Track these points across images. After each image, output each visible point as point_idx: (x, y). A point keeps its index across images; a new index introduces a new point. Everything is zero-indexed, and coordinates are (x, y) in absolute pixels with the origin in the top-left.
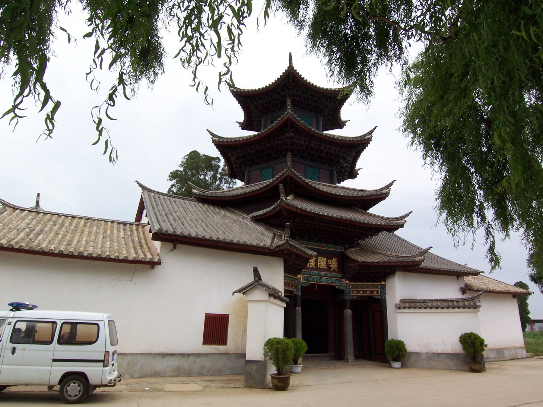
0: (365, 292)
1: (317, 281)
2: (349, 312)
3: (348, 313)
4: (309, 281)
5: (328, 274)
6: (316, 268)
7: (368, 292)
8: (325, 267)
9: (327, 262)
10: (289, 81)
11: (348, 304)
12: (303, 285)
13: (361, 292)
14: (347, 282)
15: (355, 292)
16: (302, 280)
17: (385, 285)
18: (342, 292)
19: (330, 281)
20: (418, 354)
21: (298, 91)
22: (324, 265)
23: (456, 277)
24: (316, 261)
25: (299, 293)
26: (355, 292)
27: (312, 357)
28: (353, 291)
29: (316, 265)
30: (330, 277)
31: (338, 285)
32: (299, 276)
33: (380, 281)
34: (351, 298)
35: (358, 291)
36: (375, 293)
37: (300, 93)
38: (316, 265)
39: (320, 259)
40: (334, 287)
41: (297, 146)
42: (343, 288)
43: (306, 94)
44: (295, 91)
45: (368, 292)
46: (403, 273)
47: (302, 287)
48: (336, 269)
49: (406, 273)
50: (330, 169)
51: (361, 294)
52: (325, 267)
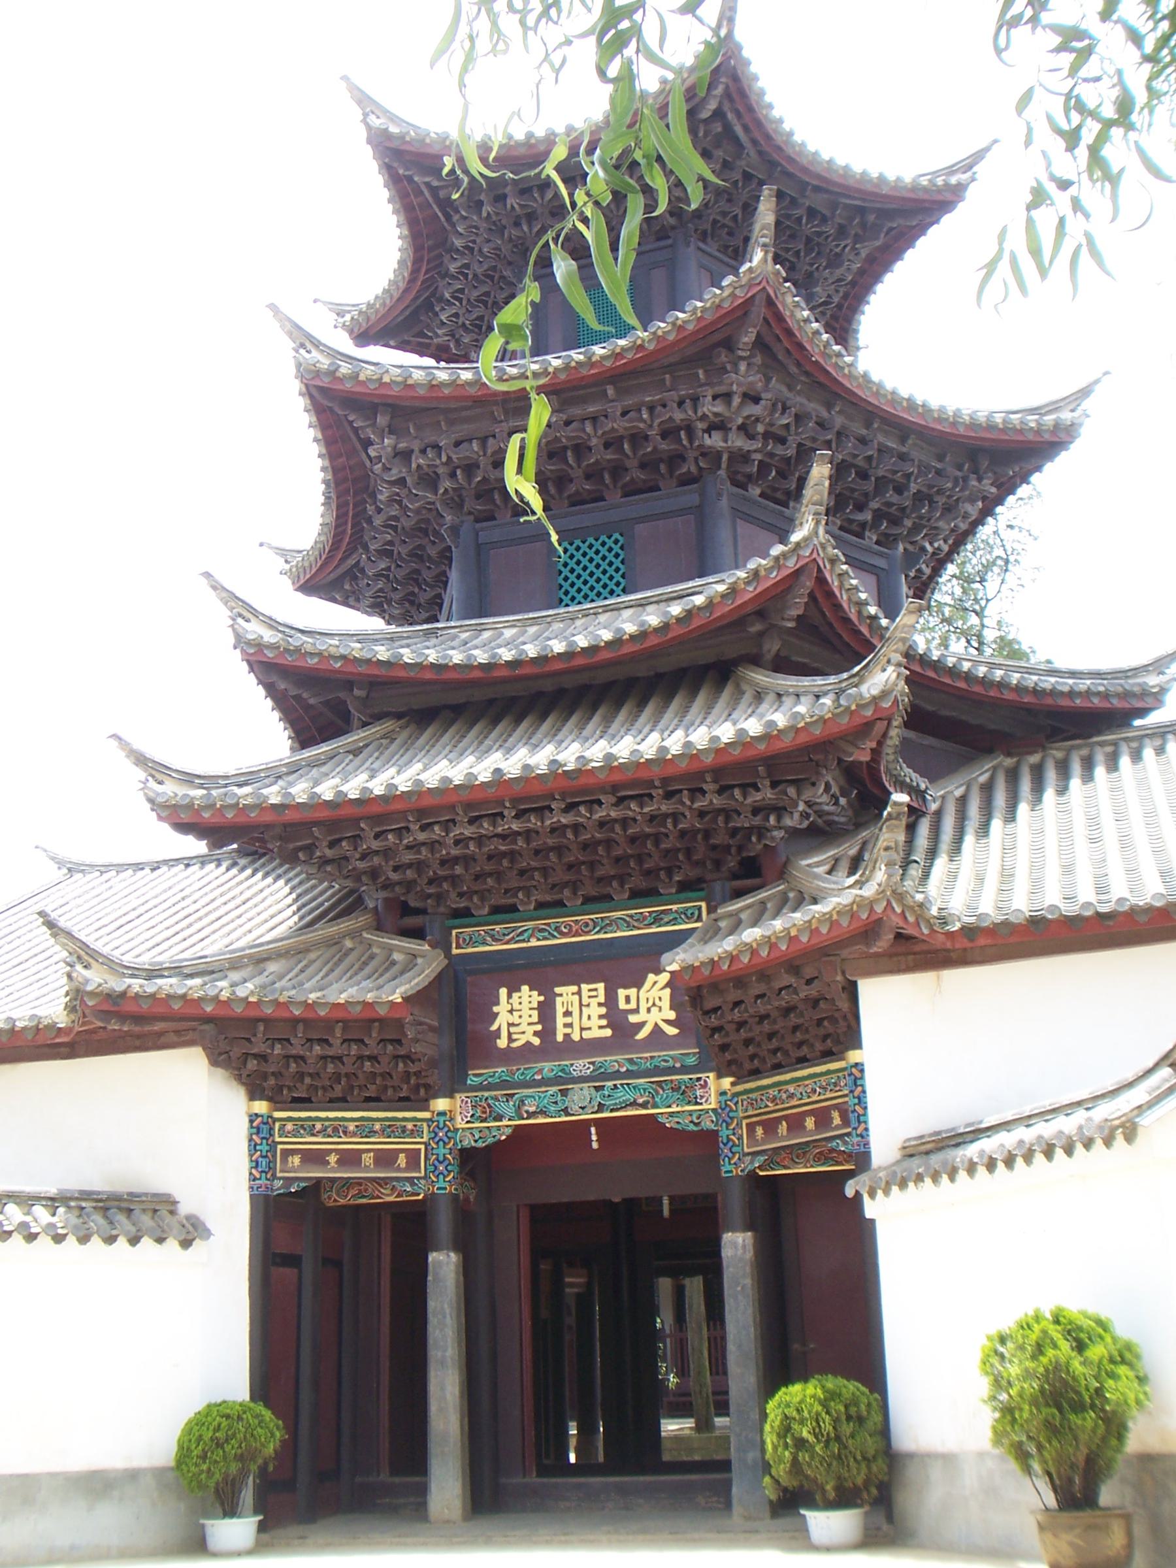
0: (796, 1123)
1: (543, 1112)
3: (727, 1253)
4: (499, 1118)
5: (614, 1061)
6: (549, 1044)
7: (810, 1123)
8: (598, 1030)
9: (610, 1001)
11: (734, 1203)
12: (468, 1142)
13: (783, 1128)
14: (727, 1082)
15: (759, 1131)
16: (460, 1123)
19: (622, 1096)
22: (596, 1022)
24: (546, 1012)
25: (445, 1184)
26: (759, 1131)
27: (622, 1491)
28: (751, 1128)
30: (630, 1074)
31: (671, 1112)
32: (441, 1104)
34: (749, 1165)
35: (770, 1127)
36: (837, 1121)
37: (511, 201)
39: (566, 995)
40: (647, 1129)
41: (453, 475)
42: (707, 1124)
44: (487, 209)
45: (810, 1123)
47: (467, 1156)
48: (672, 1031)
50: (695, 499)
51: (784, 1137)
52: (598, 1030)
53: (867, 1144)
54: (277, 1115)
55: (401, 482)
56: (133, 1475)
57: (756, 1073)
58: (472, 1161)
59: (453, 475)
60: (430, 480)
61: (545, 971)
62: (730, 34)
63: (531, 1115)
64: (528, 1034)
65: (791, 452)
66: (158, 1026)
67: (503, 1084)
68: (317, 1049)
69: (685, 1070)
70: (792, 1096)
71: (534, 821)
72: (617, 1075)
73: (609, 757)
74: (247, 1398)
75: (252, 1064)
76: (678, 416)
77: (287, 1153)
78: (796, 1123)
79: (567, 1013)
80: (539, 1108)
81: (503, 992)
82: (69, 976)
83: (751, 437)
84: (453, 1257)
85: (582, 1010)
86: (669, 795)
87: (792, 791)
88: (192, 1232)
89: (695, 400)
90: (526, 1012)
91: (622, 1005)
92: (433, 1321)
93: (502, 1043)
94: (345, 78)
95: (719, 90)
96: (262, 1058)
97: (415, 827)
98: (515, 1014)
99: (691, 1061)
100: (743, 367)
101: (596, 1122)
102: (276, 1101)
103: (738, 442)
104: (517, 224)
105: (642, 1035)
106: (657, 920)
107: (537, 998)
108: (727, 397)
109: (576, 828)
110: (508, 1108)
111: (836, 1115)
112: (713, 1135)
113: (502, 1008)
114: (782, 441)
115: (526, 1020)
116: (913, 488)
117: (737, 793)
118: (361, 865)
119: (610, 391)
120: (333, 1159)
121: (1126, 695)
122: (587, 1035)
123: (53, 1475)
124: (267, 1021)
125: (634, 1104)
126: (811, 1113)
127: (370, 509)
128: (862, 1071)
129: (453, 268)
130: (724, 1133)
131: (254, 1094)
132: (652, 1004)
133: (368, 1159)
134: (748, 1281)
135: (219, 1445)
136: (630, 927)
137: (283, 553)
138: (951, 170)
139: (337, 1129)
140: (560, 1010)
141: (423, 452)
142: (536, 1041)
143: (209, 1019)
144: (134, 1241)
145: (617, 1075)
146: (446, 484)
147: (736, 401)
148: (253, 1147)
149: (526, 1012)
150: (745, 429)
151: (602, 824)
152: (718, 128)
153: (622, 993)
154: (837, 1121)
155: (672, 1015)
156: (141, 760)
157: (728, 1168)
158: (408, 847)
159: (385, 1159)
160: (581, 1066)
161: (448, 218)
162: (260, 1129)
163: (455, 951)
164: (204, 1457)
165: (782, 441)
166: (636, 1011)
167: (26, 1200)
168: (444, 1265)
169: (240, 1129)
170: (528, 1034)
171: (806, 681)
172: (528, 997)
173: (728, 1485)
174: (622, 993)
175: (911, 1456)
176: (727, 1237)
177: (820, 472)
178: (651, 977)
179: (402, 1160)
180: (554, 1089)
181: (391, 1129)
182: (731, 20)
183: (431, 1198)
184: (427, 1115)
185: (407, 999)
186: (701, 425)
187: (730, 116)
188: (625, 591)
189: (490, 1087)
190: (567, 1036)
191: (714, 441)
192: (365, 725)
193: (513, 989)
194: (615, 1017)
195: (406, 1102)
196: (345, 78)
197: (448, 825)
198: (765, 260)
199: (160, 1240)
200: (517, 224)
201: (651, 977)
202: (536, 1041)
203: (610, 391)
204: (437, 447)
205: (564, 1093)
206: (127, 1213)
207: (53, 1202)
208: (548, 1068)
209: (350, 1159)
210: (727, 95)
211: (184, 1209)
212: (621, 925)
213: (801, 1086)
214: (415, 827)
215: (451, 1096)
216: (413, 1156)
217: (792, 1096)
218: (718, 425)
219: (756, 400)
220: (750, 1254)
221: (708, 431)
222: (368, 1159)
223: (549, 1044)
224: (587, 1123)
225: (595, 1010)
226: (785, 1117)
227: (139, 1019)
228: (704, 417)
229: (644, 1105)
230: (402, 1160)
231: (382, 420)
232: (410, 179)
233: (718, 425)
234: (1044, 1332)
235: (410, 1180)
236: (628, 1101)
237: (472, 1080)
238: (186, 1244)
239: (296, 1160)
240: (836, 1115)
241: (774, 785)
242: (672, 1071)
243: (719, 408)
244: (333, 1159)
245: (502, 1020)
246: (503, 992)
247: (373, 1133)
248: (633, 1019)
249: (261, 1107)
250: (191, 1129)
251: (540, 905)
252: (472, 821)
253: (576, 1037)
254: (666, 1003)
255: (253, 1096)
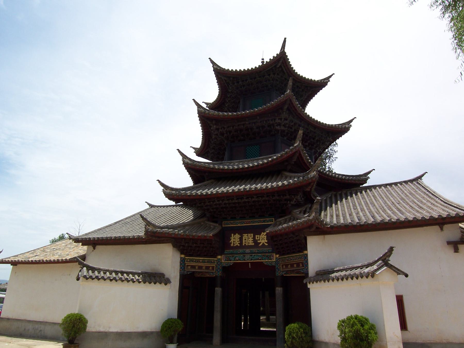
0: (292, 265)
1: (240, 260)
2: (279, 290)
3: (277, 292)
5: (255, 250)
6: (241, 246)
7: (295, 265)
8: (251, 243)
9: (254, 237)
10: (226, 80)
14: (278, 256)
15: (284, 266)
16: (223, 261)
17: (307, 255)
18: (273, 268)
20: (326, 344)
21: (238, 82)
22: (251, 242)
23: (437, 228)
24: (241, 239)
25: (219, 274)
26: (284, 266)
28: (283, 266)
29: (241, 243)
32: (219, 257)
33: (302, 252)
35: (287, 266)
36: (301, 265)
37: (240, 83)
38: (241, 243)
39: (245, 236)
41: (227, 133)
42: (273, 264)
43: (246, 80)
44: (236, 84)
45: (295, 265)
46: (322, 236)
48: (267, 244)
49: (326, 236)
51: (289, 268)
52: (251, 243)
53: (308, 271)
54: (186, 258)
55: (217, 135)
56: (152, 333)
57: (284, 254)
58: (225, 269)
59: (227, 133)
60: (222, 134)
61: (241, 231)
62: (284, 50)
63: (237, 260)
64: (237, 244)
65: (293, 130)
66: (163, 239)
67: (232, 254)
68: (195, 245)
69: (269, 253)
70: (291, 260)
71: (240, 201)
72: (255, 253)
73: (256, 188)
74: (176, 317)
75: (181, 247)
76: (271, 123)
77: (188, 266)
78: (292, 265)
79: (245, 240)
80: (239, 259)
81: (233, 235)
82: (145, 228)
83: (285, 127)
84: (220, 289)
85: (248, 239)
86: (267, 196)
87: (293, 197)
88: (167, 281)
89: (275, 120)
90: (237, 239)
91: (256, 239)
92: (216, 302)
93: (232, 245)
94: (210, 58)
95: (281, 62)
96: (184, 246)
97: (216, 201)
98: (235, 239)
99: (270, 251)
100: (284, 113)
101: (251, 262)
102: (186, 255)
103: (283, 128)
104: (241, 87)
105: (261, 245)
106: (264, 222)
107: (239, 236)
108: (281, 119)
109: (248, 202)
110: (232, 259)
111: (301, 264)
112: (274, 267)
113: (232, 238)
114: (291, 128)
115: (237, 240)
116: (316, 139)
117: (282, 197)
118: (206, 208)
119: (258, 118)
120: (197, 267)
121: (359, 180)
122: (249, 244)
123: (134, 332)
124: (185, 239)
125: (258, 259)
126: (295, 263)
127: (211, 140)
128: (307, 255)
129: (229, 96)
130: (277, 266)
131: (182, 253)
132: (263, 239)
133: (204, 268)
134: (281, 298)
135: (170, 328)
136: (258, 223)
137: (194, 148)
138: (324, 79)
139: (198, 261)
140: (244, 239)
141: (221, 129)
142: (239, 245)
143: (173, 238)
144: (155, 283)
145: (255, 253)
146: (225, 135)
147: (283, 120)
148: (181, 264)
149: (237, 239)
150: (284, 126)
151: (254, 202)
152: (280, 69)
153: (256, 236)
154: (301, 265)
155: (267, 241)
156: (162, 185)
157: (278, 274)
158: (215, 205)
159: (207, 268)
160: (248, 251)
161: (228, 86)
162: (182, 261)
163: (223, 226)
164: (166, 331)
165: (291, 128)
166: (259, 240)
167: (133, 274)
168: (218, 290)
169: (178, 260)
170: (237, 244)
171: (296, 174)
172: (237, 236)
173: (275, 341)
174: (256, 236)
175: (317, 341)
176: (277, 288)
177: (301, 132)
178: (263, 233)
179: (211, 268)
180: (242, 255)
181: (209, 262)
182: (284, 48)
183: (216, 277)
184: (216, 259)
185: (213, 235)
186: (276, 125)
187: (283, 67)
188: (259, 156)
189: (229, 254)
190: (245, 244)
191: (278, 128)
192: (208, 180)
193: (234, 234)
194: (255, 241)
195: (212, 256)
196: (210, 58)
197: (223, 200)
198: (290, 92)
199: (160, 283)
200: (241, 87)
201: (263, 233)
202: (239, 245)
203: (258, 118)
204: (224, 128)
205: (244, 256)
206: (154, 277)
207: (139, 274)
208: (241, 251)
209: (200, 267)
210: (283, 63)
211: (166, 276)
212: (257, 223)
213: (294, 257)
214: (216, 201)
215: (221, 255)
216: (213, 267)
217: (291, 260)
218: (279, 124)
219: (287, 120)
220: (281, 292)
221: (277, 126)
222: (204, 268)
223: (241, 246)
224: (249, 262)
225: (251, 239)
226: (290, 264)
227: (159, 237)
228: (276, 123)
229: (260, 260)
230: (211, 268)
231: (214, 122)
232: (221, 78)
233: (279, 124)
234: (354, 322)
235: (212, 272)
236: (257, 259)
237: (226, 252)
238: (166, 284)
239: (190, 267)
240: (301, 264)
241: (289, 195)
242: (267, 253)
243: (279, 121)
244: (197, 267)
245: (232, 240)
246: (233, 235)
247: (205, 262)
248: (259, 241)
249: (183, 256)
250: (168, 260)
251: (241, 218)
252: (228, 200)
253: (247, 245)
254: (265, 239)
255: (181, 254)
